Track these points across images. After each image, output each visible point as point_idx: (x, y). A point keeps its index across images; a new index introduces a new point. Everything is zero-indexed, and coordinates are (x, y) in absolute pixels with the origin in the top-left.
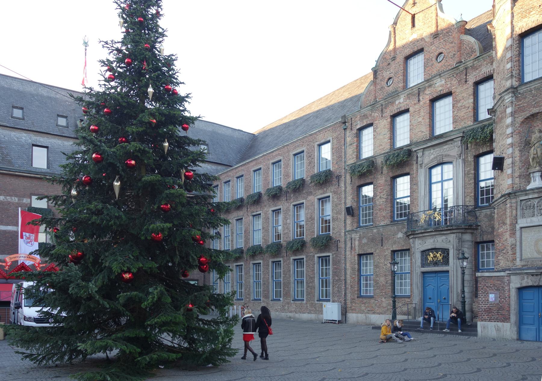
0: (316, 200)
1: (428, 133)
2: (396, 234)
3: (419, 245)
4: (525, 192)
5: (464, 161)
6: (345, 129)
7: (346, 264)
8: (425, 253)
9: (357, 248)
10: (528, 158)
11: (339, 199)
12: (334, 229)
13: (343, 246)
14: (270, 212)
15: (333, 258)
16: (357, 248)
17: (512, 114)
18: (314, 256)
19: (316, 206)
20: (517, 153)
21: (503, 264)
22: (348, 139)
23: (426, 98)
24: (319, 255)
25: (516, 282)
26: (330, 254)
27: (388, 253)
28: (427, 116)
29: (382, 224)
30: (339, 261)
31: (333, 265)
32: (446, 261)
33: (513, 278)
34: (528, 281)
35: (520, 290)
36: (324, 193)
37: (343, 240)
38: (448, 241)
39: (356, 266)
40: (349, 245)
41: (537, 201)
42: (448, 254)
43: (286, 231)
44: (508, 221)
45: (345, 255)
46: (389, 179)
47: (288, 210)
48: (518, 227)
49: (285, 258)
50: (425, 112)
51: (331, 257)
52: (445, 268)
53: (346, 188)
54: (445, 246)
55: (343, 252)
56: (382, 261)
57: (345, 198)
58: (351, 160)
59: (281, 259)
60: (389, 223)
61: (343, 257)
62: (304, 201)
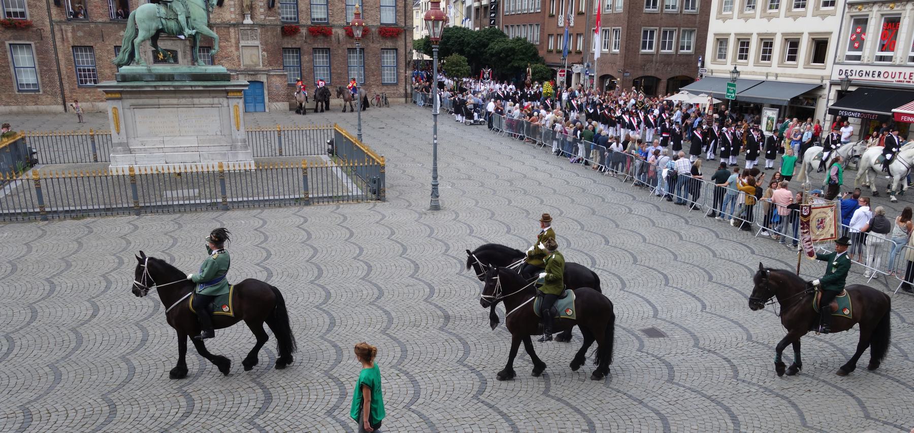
7: (56, 54)
9: (70, 40)
15: (36, 48)
16: (70, 40)
24: (11, 42)
26: (32, 43)
29: (100, 20)
30: (47, 51)
31: (38, 54)
40: (58, 36)
51: (33, 46)
55: (51, 42)
60: (108, 20)
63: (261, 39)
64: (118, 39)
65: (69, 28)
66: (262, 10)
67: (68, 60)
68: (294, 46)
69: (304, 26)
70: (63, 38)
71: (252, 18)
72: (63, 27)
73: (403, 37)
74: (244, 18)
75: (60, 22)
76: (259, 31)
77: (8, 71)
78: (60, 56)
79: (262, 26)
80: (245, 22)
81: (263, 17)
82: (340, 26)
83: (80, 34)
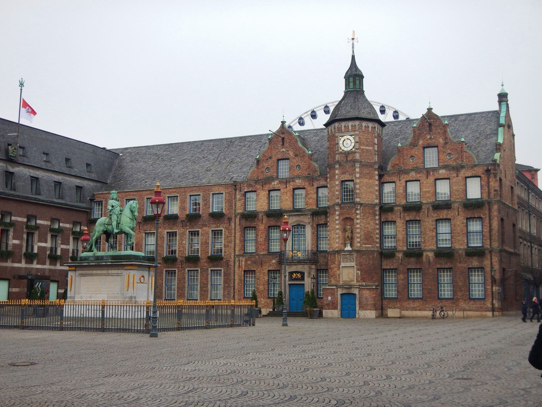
0: (210, 231)
1: (291, 206)
2: (271, 260)
3: (289, 269)
4: (344, 251)
5: (312, 226)
6: (236, 190)
7: (234, 276)
8: (291, 273)
9: (243, 266)
10: (345, 236)
11: (230, 233)
12: (225, 252)
13: (233, 264)
14: (166, 233)
15: (224, 272)
16: (243, 266)
17: (339, 215)
18: (208, 269)
19: (210, 235)
20: (341, 233)
21: (333, 282)
22: (238, 196)
23: (290, 186)
24: (212, 269)
25: (340, 292)
27: (266, 271)
28: (291, 197)
29: (262, 253)
30: (229, 274)
31: (224, 276)
32: (303, 278)
33: (339, 289)
34: (345, 291)
35: (342, 295)
36: (217, 227)
37: (232, 260)
38: (304, 268)
39: (243, 278)
40: (237, 264)
41: (348, 256)
42: (304, 275)
43: (182, 249)
44: (336, 263)
45: (234, 270)
46: (267, 227)
47: (183, 234)
48: (341, 266)
49: (180, 269)
50: (290, 194)
51: (223, 271)
52: (302, 282)
53: (235, 227)
54: (302, 270)
55: (232, 268)
56: (262, 276)
57: (235, 233)
58: (240, 211)
59: (176, 269)
61: (232, 272)
62: (200, 230)
63: (356, 261)
64: (270, 265)
65: (244, 259)
66: (359, 240)
67: (240, 280)
68: (392, 267)
69: (400, 251)
70: (239, 265)
71: (351, 246)
72: (240, 258)
73: (489, 257)
74: (345, 247)
75: (239, 256)
76: (355, 255)
77: (207, 287)
78: (236, 277)
79: (358, 251)
80: (346, 249)
81: (359, 245)
82: (431, 250)
83: (249, 262)
